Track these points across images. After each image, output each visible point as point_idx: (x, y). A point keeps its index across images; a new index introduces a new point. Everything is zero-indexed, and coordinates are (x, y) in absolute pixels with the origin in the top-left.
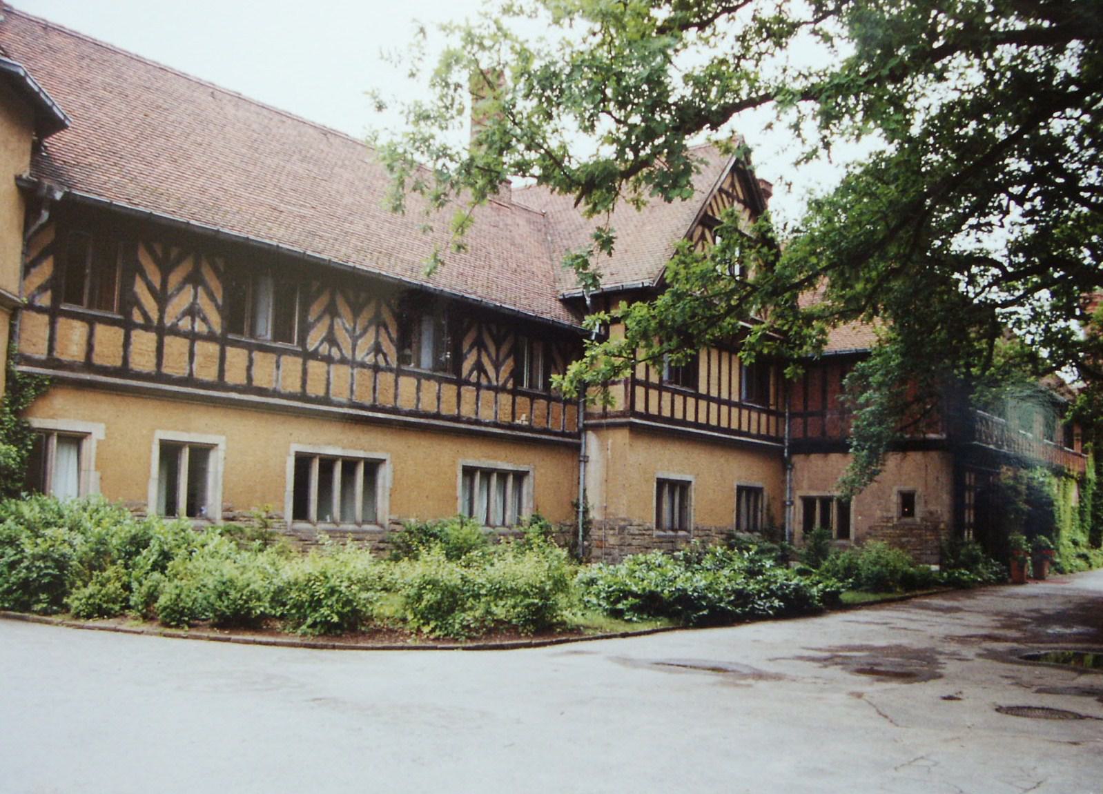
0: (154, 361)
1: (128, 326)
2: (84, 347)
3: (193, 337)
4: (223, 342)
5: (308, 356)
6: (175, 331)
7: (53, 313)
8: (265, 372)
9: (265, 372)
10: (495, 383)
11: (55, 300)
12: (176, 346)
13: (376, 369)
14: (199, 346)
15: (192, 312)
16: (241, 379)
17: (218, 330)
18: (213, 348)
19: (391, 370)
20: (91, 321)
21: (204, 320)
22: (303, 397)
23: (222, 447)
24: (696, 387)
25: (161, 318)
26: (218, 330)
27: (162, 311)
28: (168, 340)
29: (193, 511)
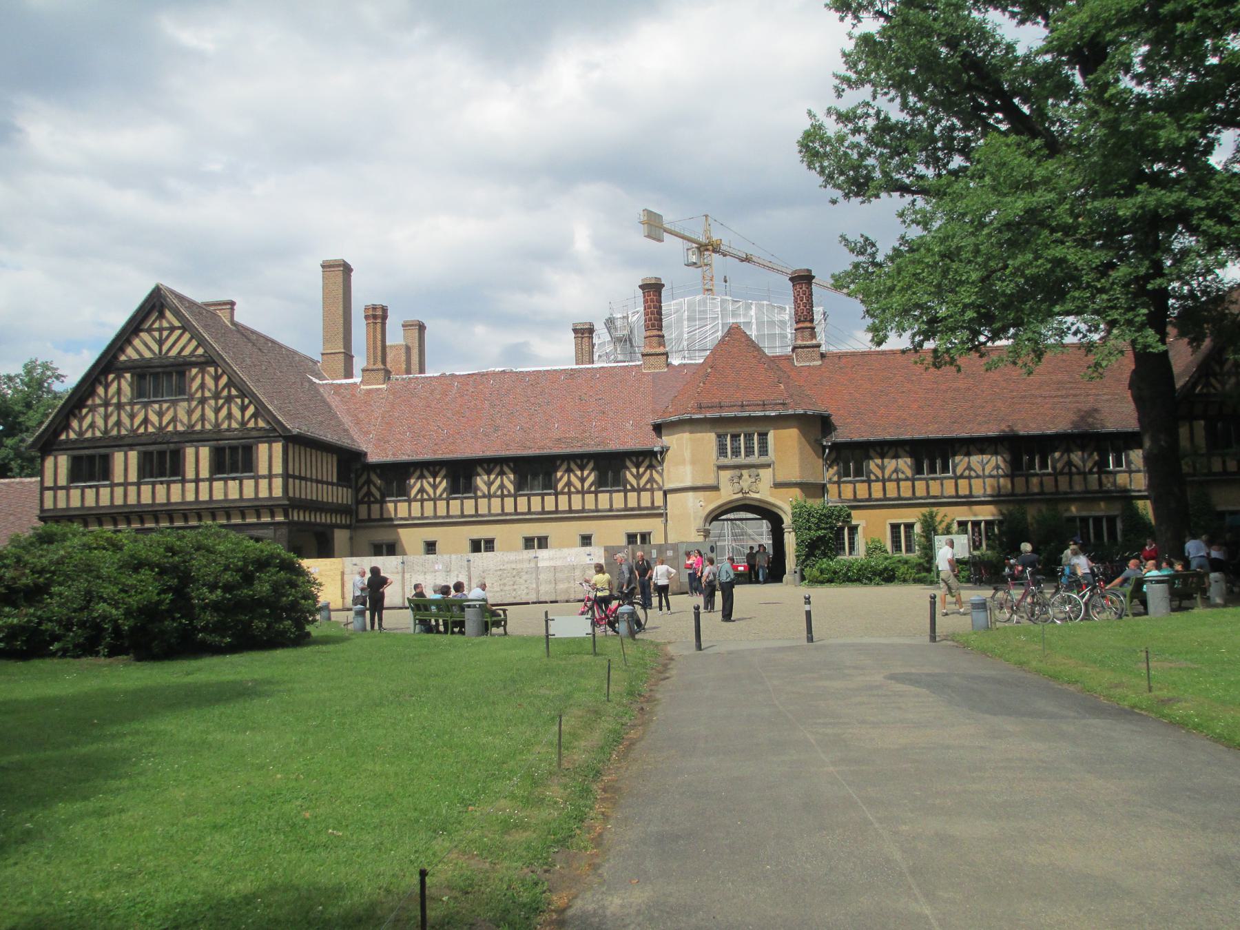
1: (869, 482)
5: (956, 478)
6: (890, 480)
7: (838, 483)
8: (935, 488)
9: (935, 488)
11: (839, 478)
15: (896, 471)
18: (909, 483)
20: (854, 483)
27: (883, 473)
29: (909, 549)
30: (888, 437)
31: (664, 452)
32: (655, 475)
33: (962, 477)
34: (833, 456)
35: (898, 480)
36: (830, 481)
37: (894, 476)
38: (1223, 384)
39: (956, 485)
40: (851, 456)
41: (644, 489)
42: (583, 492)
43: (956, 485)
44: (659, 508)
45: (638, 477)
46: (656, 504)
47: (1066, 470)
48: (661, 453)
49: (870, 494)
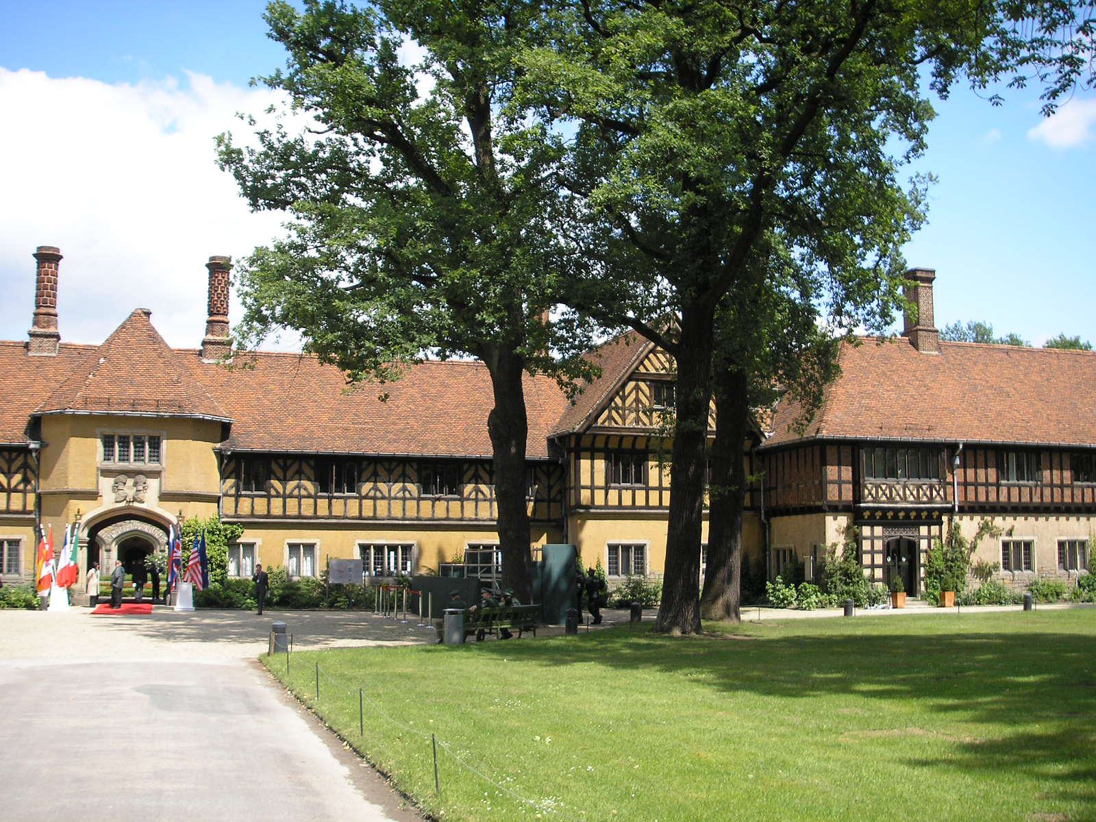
0: (282, 510)
1: (269, 497)
2: (250, 508)
3: (300, 497)
4: (316, 497)
5: (361, 498)
6: (291, 496)
10: (489, 496)
11: (238, 490)
12: (292, 503)
13: (404, 499)
14: (303, 500)
16: (326, 513)
17: (313, 493)
19: (414, 499)
20: (252, 497)
21: (305, 489)
22: (360, 518)
23: (318, 544)
24: (646, 483)
25: (284, 492)
26: (313, 493)
27: (285, 488)
28: (288, 500)
30: (292, 450)
33: (366, 497)
34: (232, 465)
36: (226, 495)
37: (296, 492)
38: (624, 418)
39: (361, 505)
40: (250, 469)
41: (15, 490)
43: (361, 505)
44: (30, 512)
47: (473, 496)
49: (269, 511)
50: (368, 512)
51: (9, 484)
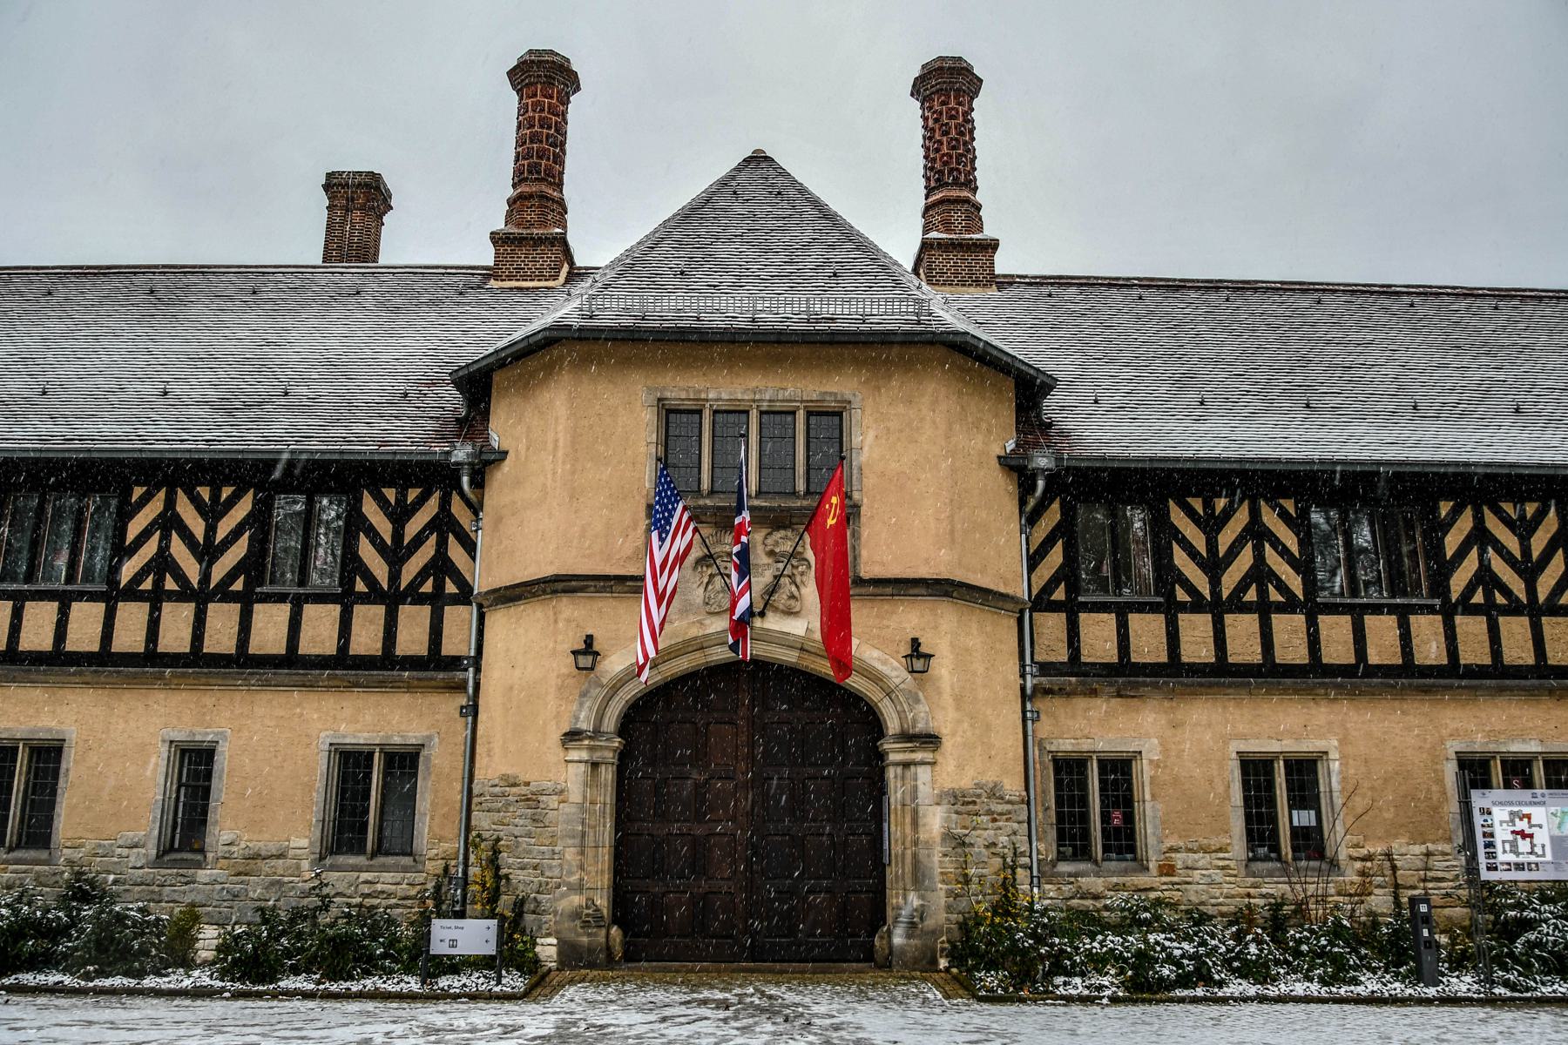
1: (1171, 610)
14: (1277, 619)
23: (1334, 755)
27: (1215, 583)
28: (1229, 619)
31: (485, 464)
32: (456, 552)
35: (1264, 610)
42: (200, 597)
44: (455, 663)
45: (396, 555)
46: (449, 648)
48: (479, 483)
50: (1474, 651)
51: (394, 577)
